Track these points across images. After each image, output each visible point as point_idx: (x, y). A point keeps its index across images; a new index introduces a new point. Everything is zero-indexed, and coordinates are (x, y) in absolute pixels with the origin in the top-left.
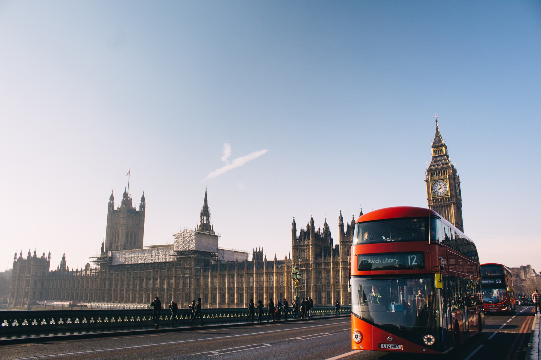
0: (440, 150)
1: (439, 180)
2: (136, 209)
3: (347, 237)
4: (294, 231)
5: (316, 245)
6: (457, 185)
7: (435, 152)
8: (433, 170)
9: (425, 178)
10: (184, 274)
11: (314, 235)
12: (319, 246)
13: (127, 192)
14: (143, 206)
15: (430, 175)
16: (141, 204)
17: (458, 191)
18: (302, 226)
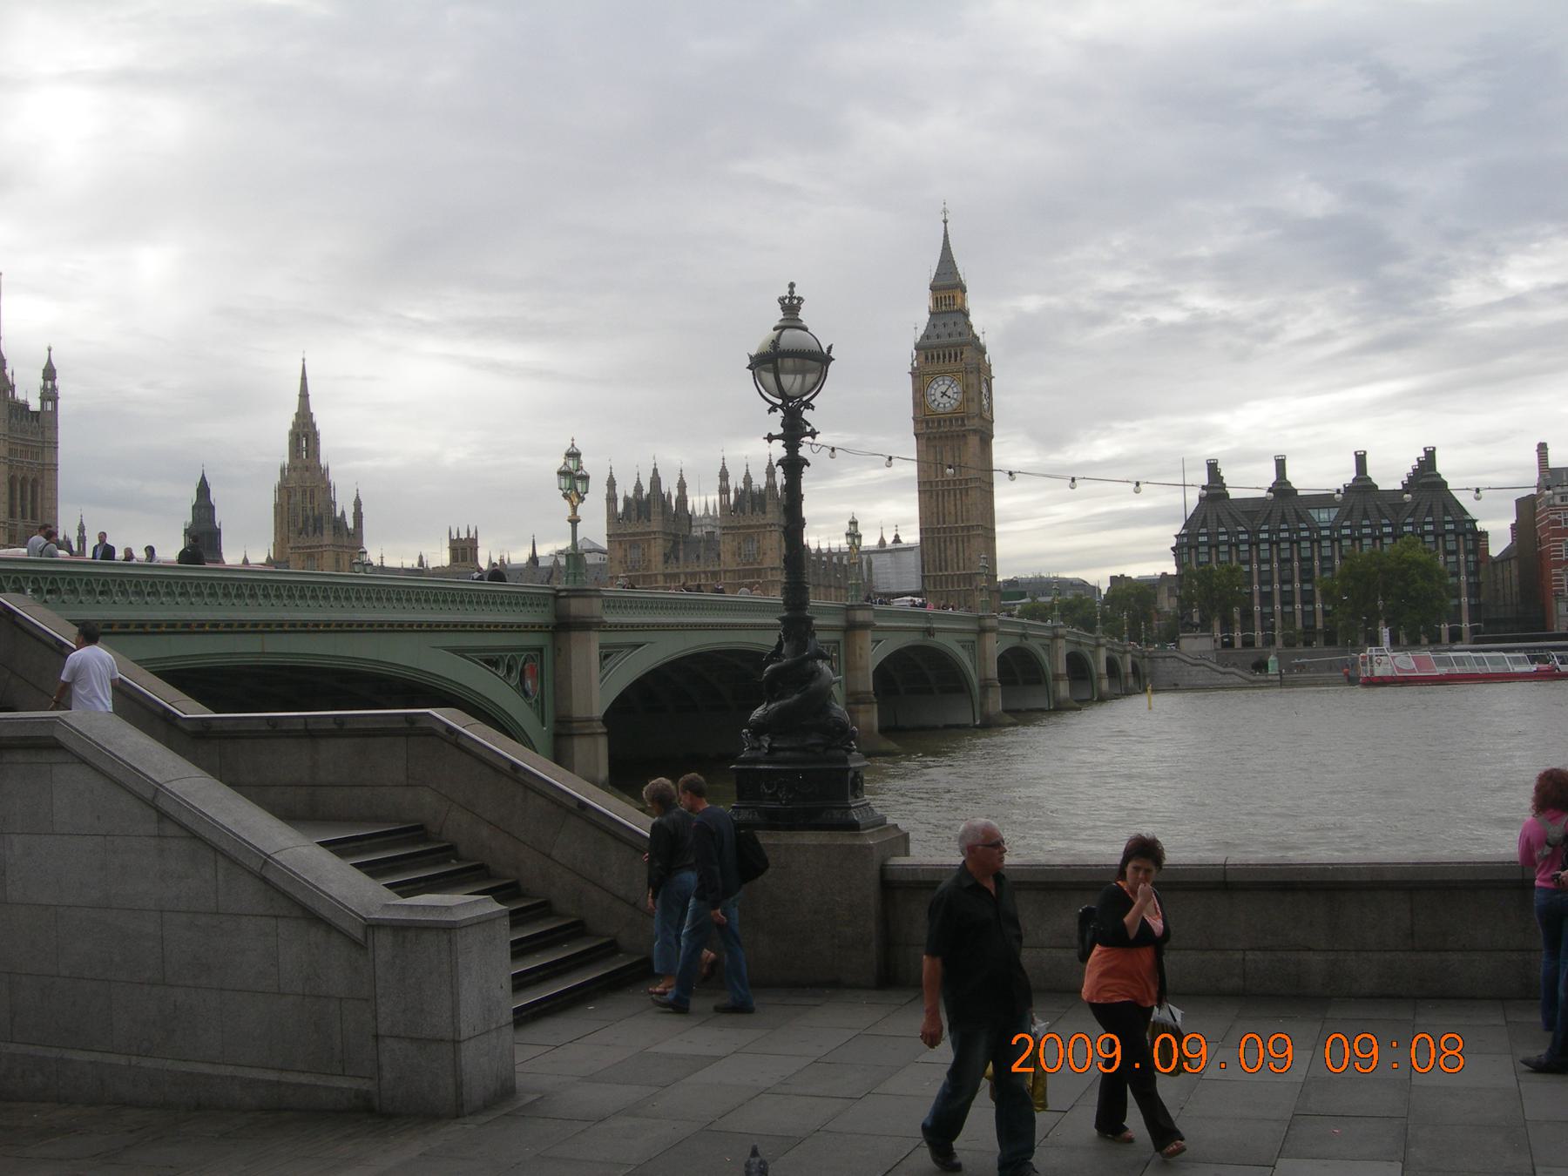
0: (949, 297)
1: (943, 374)
2: (25, 406)
3: (738, 516)
5: (665, 533)
6: (984, 385)
7: (936, 301)
8: (932, 347)
9: (910, 367)
11: (660, 510)
12: (671, 534)
14: (50, 395)
15: (922, 358)
16: (44, 388)
17: (985, 402)
18: (625, 489)
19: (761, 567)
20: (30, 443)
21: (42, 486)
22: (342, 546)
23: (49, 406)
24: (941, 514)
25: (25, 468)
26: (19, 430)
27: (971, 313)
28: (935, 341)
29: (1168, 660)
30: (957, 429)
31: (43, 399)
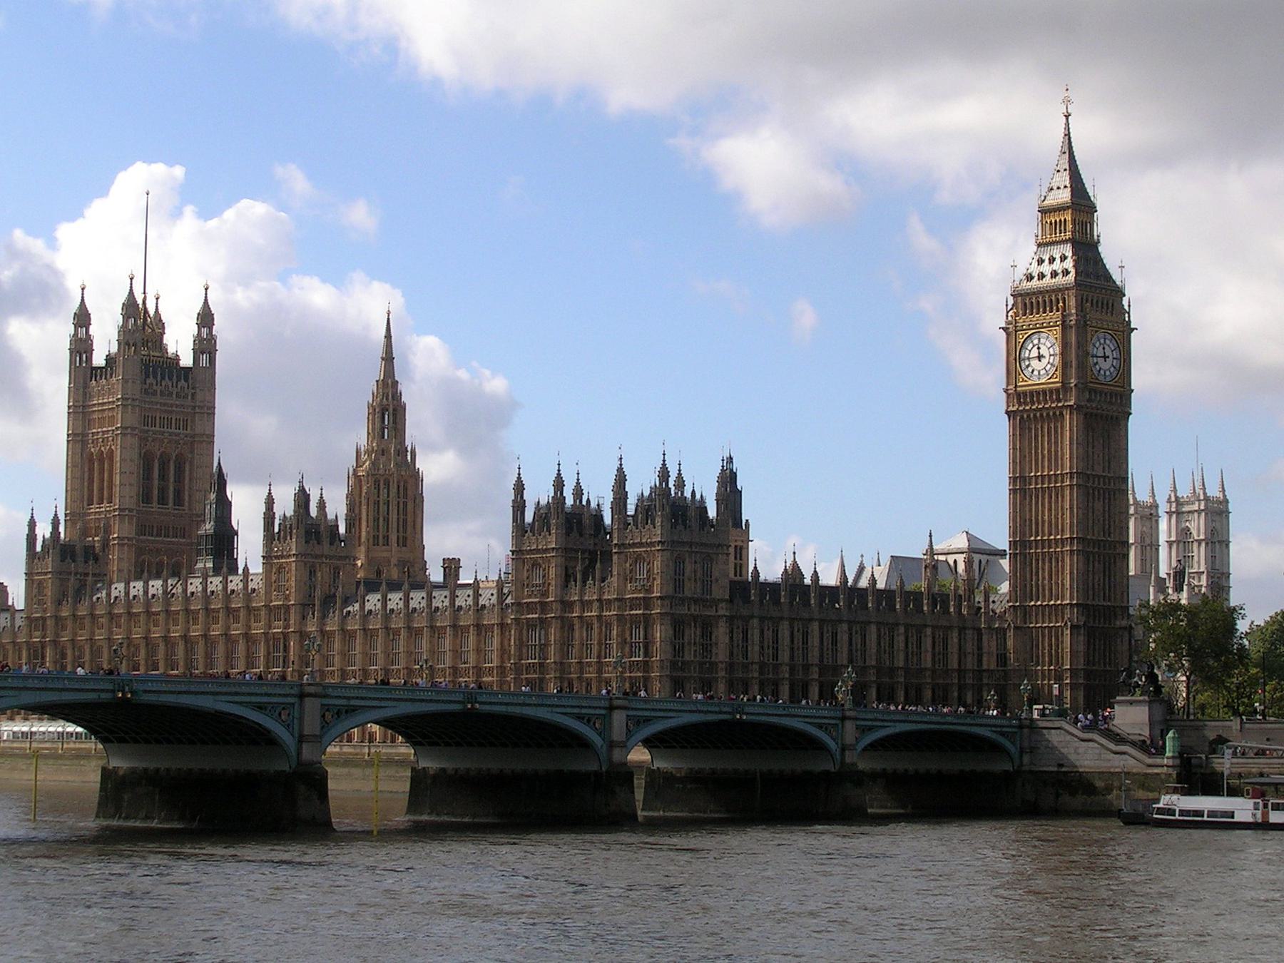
0: (1060, 220)
1: (1038, 329)
4: (519, 506)
10: (270, 628)
13: (139, 299)
14: (205, 346)
19: (650, 596)
20: (174, 409)
21: (191, 464)
22: (322, 556)
23: (204, 360)
24: (1034, 521)
25: (166, 441)
26: (159, 392)
27: (1101, 241)
28: (1035, 283)
29: (1053, 731)
30: (1053, 405)
31: (197, 352)
